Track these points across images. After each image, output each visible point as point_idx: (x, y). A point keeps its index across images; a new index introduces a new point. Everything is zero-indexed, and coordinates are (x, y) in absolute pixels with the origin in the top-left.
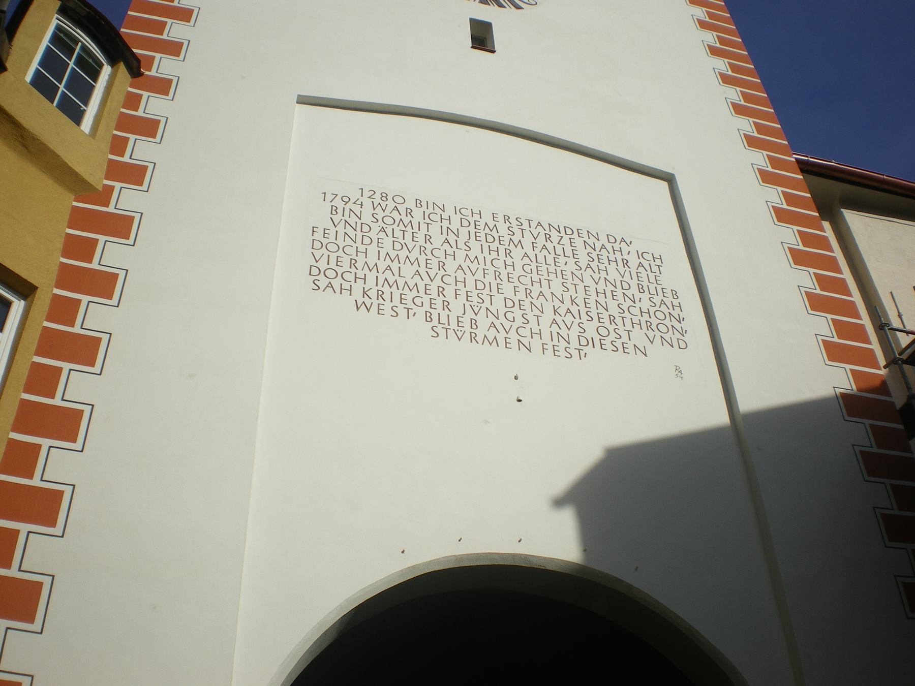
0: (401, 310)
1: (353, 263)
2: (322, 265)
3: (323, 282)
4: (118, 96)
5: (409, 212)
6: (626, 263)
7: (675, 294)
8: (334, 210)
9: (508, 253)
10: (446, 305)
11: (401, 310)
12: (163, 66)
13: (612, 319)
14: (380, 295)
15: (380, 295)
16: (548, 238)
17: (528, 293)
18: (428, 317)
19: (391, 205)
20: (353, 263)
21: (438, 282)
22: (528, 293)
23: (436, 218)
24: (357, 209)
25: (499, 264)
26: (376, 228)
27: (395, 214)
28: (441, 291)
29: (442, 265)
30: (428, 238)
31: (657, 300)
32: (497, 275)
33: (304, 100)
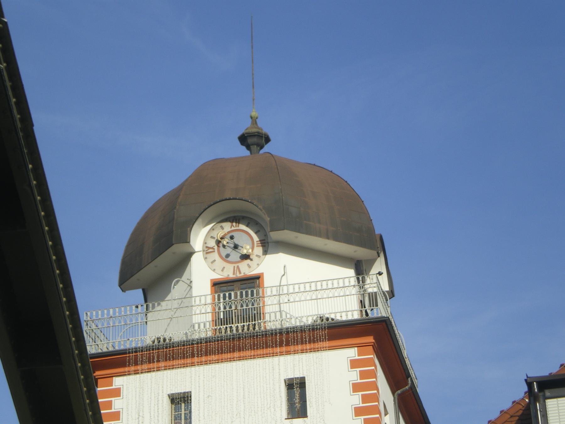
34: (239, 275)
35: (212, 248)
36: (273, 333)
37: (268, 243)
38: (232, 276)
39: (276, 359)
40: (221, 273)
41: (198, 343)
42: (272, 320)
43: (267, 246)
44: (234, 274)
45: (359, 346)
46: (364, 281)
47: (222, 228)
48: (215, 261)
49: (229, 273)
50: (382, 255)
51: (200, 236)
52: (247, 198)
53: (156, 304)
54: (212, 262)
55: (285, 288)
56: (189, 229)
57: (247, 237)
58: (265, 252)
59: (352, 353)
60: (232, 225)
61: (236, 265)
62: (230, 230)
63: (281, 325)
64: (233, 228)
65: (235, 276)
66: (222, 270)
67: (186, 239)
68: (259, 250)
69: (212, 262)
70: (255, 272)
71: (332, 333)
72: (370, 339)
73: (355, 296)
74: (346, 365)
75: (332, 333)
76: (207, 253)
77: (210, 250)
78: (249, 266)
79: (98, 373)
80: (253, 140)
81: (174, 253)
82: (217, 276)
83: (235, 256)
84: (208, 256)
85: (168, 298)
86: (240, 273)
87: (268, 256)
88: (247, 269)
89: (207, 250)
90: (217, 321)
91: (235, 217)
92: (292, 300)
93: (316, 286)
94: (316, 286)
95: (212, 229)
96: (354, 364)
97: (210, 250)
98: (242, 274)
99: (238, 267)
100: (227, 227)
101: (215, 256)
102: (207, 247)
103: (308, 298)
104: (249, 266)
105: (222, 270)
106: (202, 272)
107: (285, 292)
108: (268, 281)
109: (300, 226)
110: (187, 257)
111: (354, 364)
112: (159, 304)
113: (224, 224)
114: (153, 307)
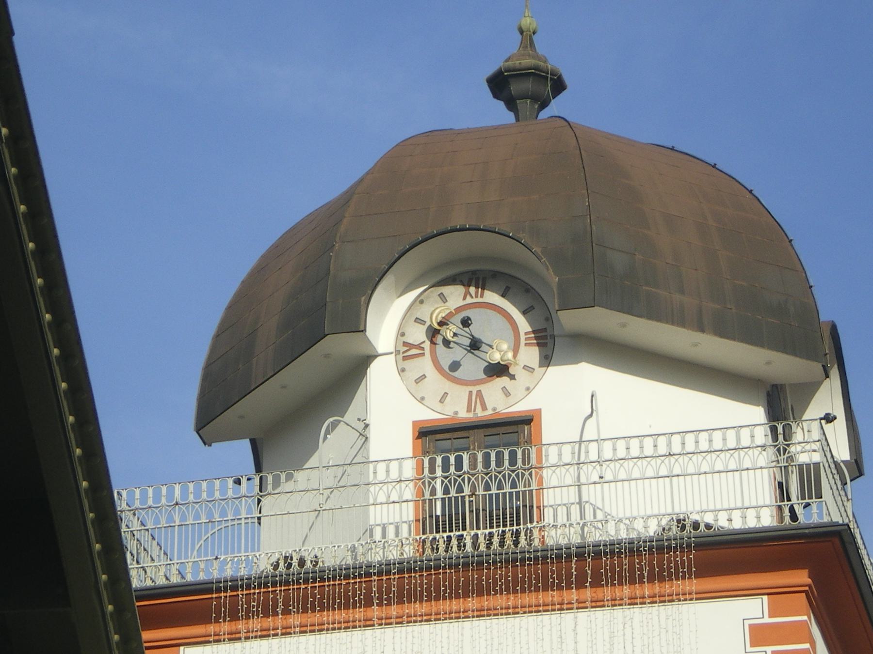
34: (481, 414)
35: (419, 347)
36: (562, 556)
37: (553, 337)
38: (464, 415)
39: (568, 617)
40: (439, 407)
41: (380, 573)
42: (560, 524)
43: (551, 344)
44: (469, 410)
45: (772, 592)
46: (788, 435)
47: (443, 298)
48: (424, 377)
49: (457, 407)
50: (835, 373)
51: (389, 318)
52: (505, 228)
53: (283, 476)
54: (417, 381)
55: (593, 447)
57: (503, 323)
58: (546, 360)
59: (755, 609)
60: (467, 294)
62: (462, 303)
63: (583, 536)
64: (469, 300)
65: (471, 415)
66: (441, 401)
67: (356, 325)
68: (530, 355)
69: (417, 381)
70: (521, 407)
71: (702, 558)
72: (802, 577)
73: (765, 471)
75: (702, 558)
76: (405, 358)
78: (506, 393)
79: (146, 635)
80: (524, 85)
81: (327, 356)
82: (428, 415)
83: (472, 367)
85: (313, 462)
86: (484, 408)
87: (553, 371)
88: (499, 400)
89: (407, 352)
90: (428, 522)
91: (474, 272)
92: (609, 477)
93: (669, 444)
94: (669, 444)
95: (420, 301)
98: (489, 412)
99: (479, 392)
100: (456, 296)
101: (425, 365)
102: (405, 344)
103: (650, 473)
104: (506, 393)
105: (441, 401)
107: (593, 456)
108: (552, 430)
109: (630, 298)
110: (357, 368)
112: (289, 477)
113: (447, 290)
114: (277, 483)
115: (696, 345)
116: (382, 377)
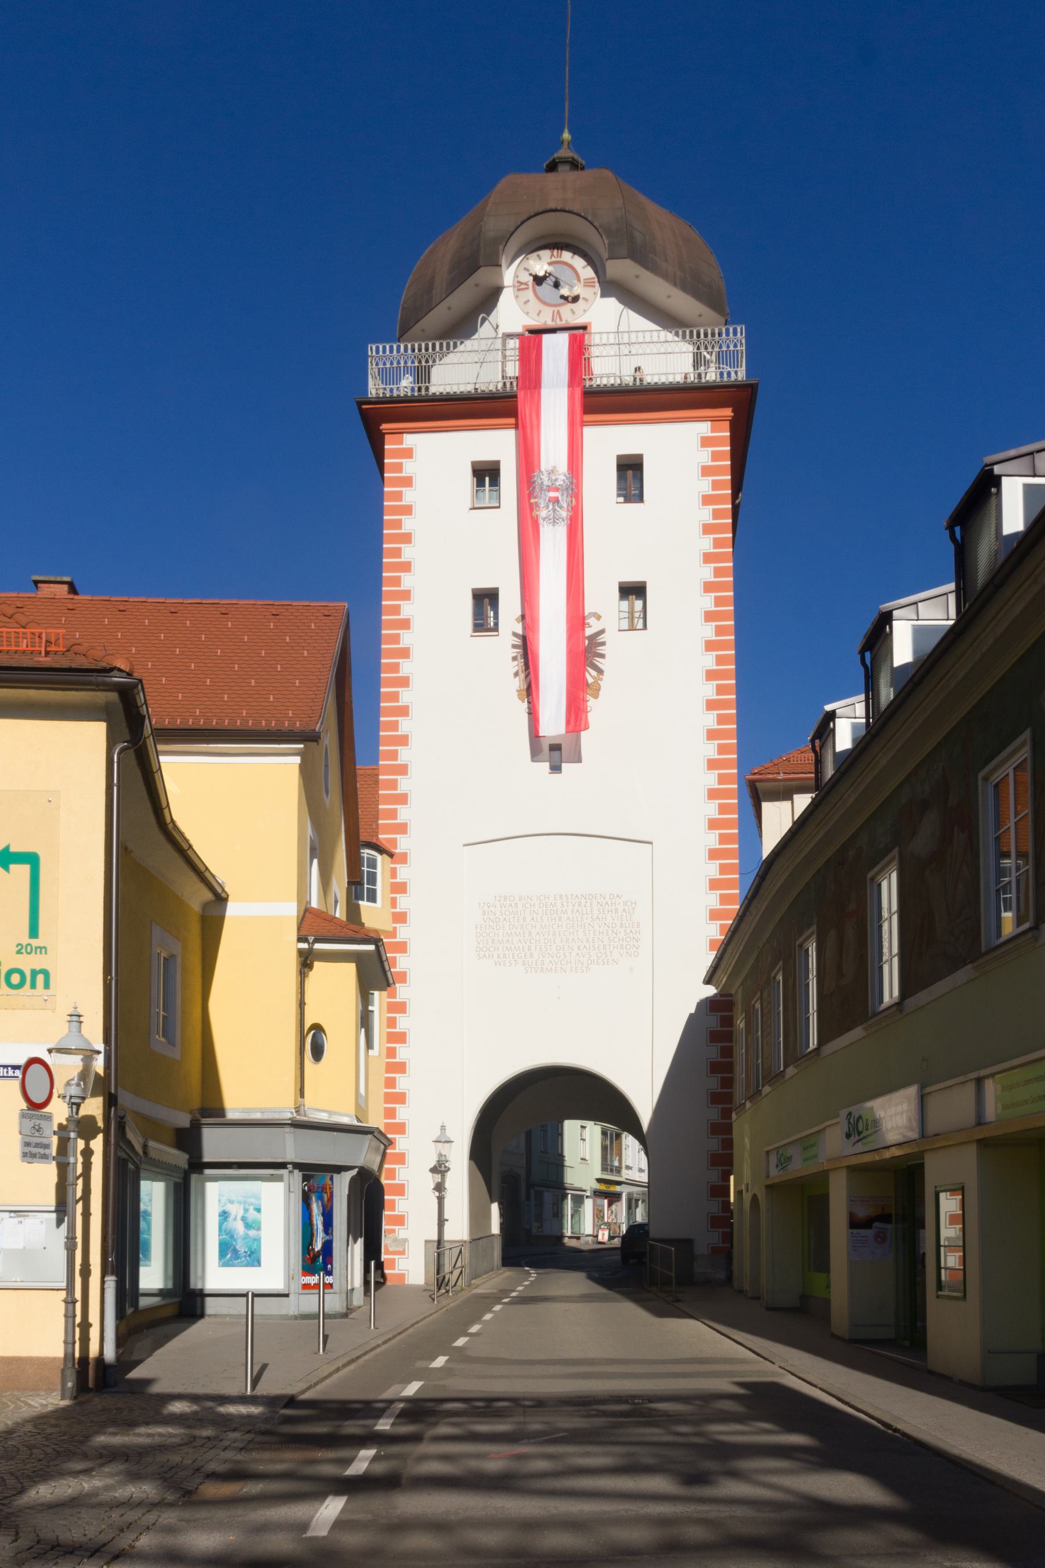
0: (513, 962)
1: (493, 942)
2: (481, 945)
3: (482, 953)
4: (388, 874)
5: (516, 905)
6: (616, 910)
7: (638, 925)
8: (484, 912)
9: (560, 919)
10: (531, 955)
11: (513, 962)
12: (403, 844)
13: (605, 946)
14: (504, 956)
15: (504, 956)
16: (580, 904)
17: (567, 941)
18: (524, 964)
19: (508, 902)
20: (493, 942)
21: (528, 943)
22: (567, 940)
23: (528, 905)
24: (493, 909)
25: (555, 926)
26: (502, 918)
27: (510, 909)
28: (529, 949)
29: (530, 933)
30: (524, 919)
31: (628, 931)
32: (554, 934)
33: (465, 845)
34: (559, 324)
35: (526, 284)
40: (536, 318)
44: (553, 320)
45: (714, 420)
52: (579, 212)
55: (626, 335)
56: (501, 247)
59: (704, 428)
60: (552, 255)
61: (556, 309)
64: (553, 259)
66: (538, 314)
72: (728, 412)
74: (696, 442)
76: (519, 290)
77: (523, 286)
78: (573, 312)
84: (521, 292)
85: (476, 336)
86: (561, 320)
92: (633, 352)
96: (705, 442)
97: (523, 286)
99: (558, 312)
101: (529, 294)
104: (573, 312)
105: (538, 314)
106: (512, 313)
107: (626, 340)
111: (705, 442)
112: (462, 343)
113: (542, 253)
114: (455, 347)
115: (669, 297)
116: (507, 300)
